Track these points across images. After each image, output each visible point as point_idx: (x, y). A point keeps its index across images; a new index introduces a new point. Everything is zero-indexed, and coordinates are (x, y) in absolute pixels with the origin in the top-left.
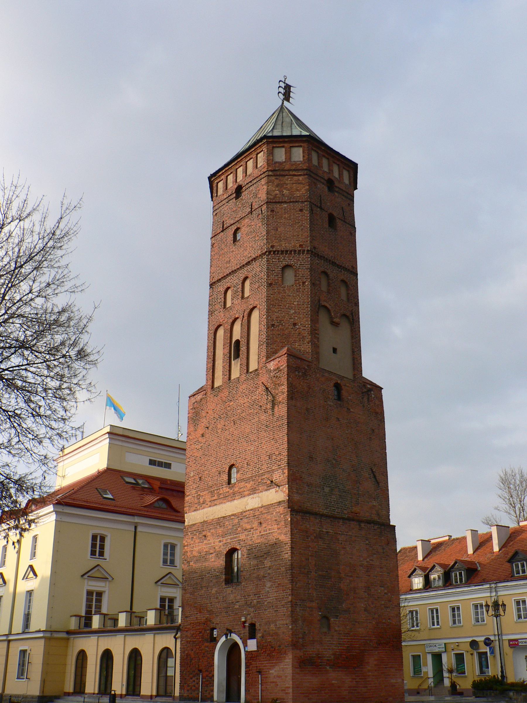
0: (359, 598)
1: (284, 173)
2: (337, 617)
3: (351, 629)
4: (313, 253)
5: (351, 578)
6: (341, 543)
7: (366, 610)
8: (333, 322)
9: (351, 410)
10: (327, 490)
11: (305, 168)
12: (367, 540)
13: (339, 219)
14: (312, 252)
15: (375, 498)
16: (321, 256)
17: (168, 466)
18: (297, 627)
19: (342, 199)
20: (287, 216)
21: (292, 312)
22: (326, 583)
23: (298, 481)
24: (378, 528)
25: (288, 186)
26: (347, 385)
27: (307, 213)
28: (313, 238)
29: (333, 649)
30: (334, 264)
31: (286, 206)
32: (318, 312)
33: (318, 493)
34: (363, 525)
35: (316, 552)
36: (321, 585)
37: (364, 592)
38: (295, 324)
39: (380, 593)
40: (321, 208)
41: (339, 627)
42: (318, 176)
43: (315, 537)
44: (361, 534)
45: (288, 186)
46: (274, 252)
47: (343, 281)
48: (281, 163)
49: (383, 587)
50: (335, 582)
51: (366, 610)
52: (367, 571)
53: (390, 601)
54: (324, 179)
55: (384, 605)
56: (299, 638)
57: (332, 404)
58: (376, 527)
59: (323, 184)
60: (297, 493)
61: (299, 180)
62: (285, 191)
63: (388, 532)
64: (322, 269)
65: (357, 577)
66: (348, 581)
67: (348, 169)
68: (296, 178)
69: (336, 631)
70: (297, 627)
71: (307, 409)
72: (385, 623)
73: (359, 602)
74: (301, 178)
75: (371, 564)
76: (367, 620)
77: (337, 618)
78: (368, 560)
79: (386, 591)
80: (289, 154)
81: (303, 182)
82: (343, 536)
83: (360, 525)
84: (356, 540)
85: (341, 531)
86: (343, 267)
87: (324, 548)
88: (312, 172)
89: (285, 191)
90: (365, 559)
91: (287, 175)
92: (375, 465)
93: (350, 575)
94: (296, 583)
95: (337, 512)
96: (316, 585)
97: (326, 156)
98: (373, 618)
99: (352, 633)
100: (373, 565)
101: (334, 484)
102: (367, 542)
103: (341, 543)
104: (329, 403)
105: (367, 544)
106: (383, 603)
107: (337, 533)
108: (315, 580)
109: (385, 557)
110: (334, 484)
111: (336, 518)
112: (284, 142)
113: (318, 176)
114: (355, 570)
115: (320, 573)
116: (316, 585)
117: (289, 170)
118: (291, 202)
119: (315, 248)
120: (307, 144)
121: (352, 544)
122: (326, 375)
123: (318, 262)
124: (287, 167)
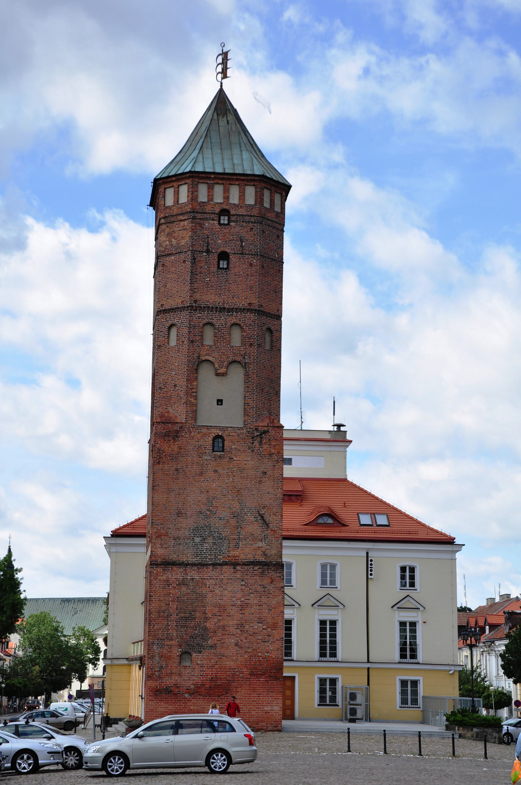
0: (229, 635)
1: (172, 219)
2: (200, 652)
3: (217, 662)
4: (194, 308)
5: (220, 618)
6: (209, 587)
7: (236, 645)
10: (197, 540)
11: (189, 210)
13: (235, 253)
14: (193, 306)
15: (262, 540)
16: (204, 307)
18: (153, 662)
19: (242, 226)
20: (173, 269)
21: (174, 373)
22: (189, 624)
23: (162, 537)
24: (259, 568)
25: (176, 235)
26: (233, 434)
27: (188, 263)
28: (193, 291)
29: (193, 680)
30: (222, 310)
31: (173, 258)
32: (197, 370)
34: (238, 568)
35: (177, 597)
38: (175, 386)
39: (257, 629)
40: (208, 251)
41: (201, 660)
42: (206, 213)
43: (177, 585)
44: (236, 577)
45: (176, 235)
46: (164, 310)
47: (235, 324)
48: (169, 208)
49: (261, 623)
51: (236, 645)
52: (241, 610)
53: (270, 636)
54: (215, 213)
55: (260, 639)
56: (155, 671)
57: (209, 458)
58: (256, 568)
59: (213, 220)
60: (162, 547)
61: (184, 226)
62: (173, 240)
63: (273, 571)
64: (206, 321)
66: (216, 620)
67: (252, 183)
68: (182, 223)
69: (198, 664)
70: (153, 662)
71: (177, 470)
72: (261, 656)
73: (228, 639)
74: (186, 223)
76: (237, 654)
77: (200, 653)
78: (243, 599)
79: (265, 627)
80: (177, 194)
81: (188, 227)
82: (211, 581)
83: (235, 568)
84: (228, 583)
86: (236, 309)
87: (188, 593)
88: (197, 212)
89: (173, 240)
91: (175, 221)
92: (264, 507)
94: (154, 626)
95: (209, 559)
96: (176, 626)
97: (220, 182)
98: (246, 652)
99: (217, 666)
100: (249, 604)
101: (207, 533)
102: (243, 583)
103: (209, 587)
104: (205, 458)
105: (242, 585)
106: (260, 637)
107: (204, 579)
109: (266, 595)
110: (207, 533)
111: (204, 565)
112: (172, 181)
113: (206, 213)
115: (183, 615)
116: (176, 626)
117: (177, 215)
118: (176, 253)
119: (196, 301)
120: (191, 179)
121: (222, 587)
122: (204, 431)
123: (200, 315)
124: (175, 211)
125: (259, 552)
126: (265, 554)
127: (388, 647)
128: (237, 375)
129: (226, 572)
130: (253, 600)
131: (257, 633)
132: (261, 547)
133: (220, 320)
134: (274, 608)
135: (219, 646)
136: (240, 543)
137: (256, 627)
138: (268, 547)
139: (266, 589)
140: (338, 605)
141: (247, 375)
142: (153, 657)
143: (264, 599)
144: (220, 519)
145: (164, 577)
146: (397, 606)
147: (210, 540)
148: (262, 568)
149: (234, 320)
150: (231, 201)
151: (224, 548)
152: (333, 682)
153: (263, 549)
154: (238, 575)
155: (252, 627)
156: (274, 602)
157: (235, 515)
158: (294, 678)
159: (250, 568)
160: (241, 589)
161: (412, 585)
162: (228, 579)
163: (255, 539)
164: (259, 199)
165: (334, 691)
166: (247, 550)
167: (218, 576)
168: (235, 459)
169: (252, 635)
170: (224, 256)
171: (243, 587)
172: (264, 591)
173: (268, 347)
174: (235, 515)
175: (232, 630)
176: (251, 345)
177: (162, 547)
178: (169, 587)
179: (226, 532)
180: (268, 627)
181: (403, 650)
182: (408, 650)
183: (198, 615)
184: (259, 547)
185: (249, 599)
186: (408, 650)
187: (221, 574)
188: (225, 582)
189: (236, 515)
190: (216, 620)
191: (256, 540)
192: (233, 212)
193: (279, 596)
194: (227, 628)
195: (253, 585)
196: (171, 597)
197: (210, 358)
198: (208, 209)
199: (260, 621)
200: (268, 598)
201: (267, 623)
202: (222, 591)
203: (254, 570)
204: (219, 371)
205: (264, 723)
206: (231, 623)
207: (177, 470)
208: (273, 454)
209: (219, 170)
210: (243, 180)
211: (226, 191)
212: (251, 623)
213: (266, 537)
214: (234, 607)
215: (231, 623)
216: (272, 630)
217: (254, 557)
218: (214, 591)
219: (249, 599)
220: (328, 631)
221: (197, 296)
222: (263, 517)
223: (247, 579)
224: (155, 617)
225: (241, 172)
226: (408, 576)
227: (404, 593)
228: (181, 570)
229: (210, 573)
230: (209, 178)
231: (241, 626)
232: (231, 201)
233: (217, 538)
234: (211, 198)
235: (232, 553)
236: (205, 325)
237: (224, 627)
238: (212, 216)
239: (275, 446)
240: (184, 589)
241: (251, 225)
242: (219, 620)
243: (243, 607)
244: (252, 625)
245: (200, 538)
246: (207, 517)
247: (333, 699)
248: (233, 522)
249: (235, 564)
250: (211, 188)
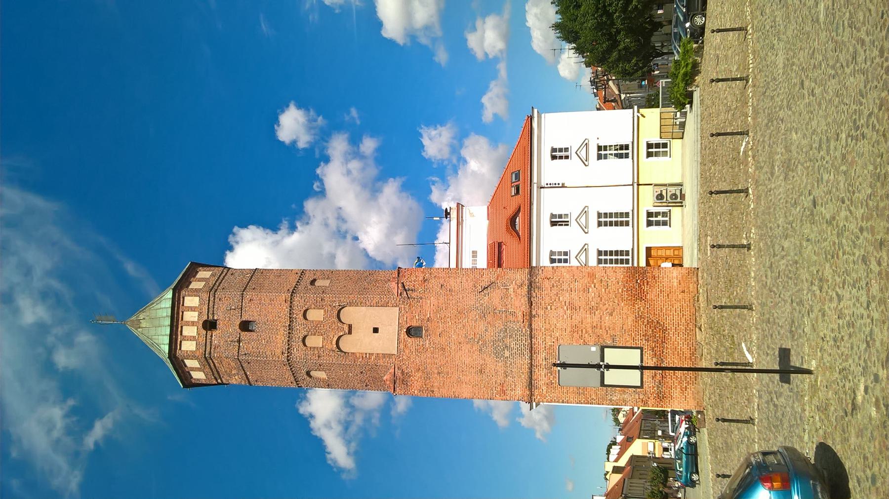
10: (507, 354)
17: (474, 254)
34: (534, 313)
40: (239, 341)
58: (534, 295)
64: (301, 344)
71: (439, 373)
80: (194, 369)
122: (402, 346)
124: (208, 370)
127: (619, 170)
128: (350, 314)
130: (566, 297)
133: (300, 330)
135: (612, 332)
140: (585, 212)
141: (350, 304)
142: (624, 401)
143: (565, 287)
145: (544, 388)
146: (585, 162)
147: (508, 340)
149: (301, 316)
150: (196, 319)
152: (649, 214)
154: (541, 312)
156: (568, 276)
157: (483, 316)
158: (649, 249)
161: (566, 149)
163: (506, 296)
164: (196, 292)
165: (657, 214)
166: (517, 304)
170: (245, 326)
173: (326, 283)
174: (483, 316)
175: (596, 319)
179: (499, 325)
181: (620, 156)
182: (622, 152)
186: (622, 152)
188: (548, 326)
192: (205, 318)
197: (335, 339)
198: (202, 340)
199: (586, 290)
204: (347, 331)
205: (691, 286)
206: (589, 320)
207: (439, 373)
209: (168, 332)
210: (178, 308)
211: (188, 324)
213: (505, 285)
215: (589, 320)
220: (608, 220)
225: (170, 310)
226: (558, 154)
227: (574, 156)
229: (539, 341)
231: (592, 310)
232: (196, 319)
234: (192, 338)
235: (520, 318)
236: (305, 345)
237: (593, 327)
238: (209, 337)
242: (586, 332)
243: (572, 307)
246: (484, 344)
247: (664, 214)
248: (489, 318)
249: (531, 316)
250: (186, 338)
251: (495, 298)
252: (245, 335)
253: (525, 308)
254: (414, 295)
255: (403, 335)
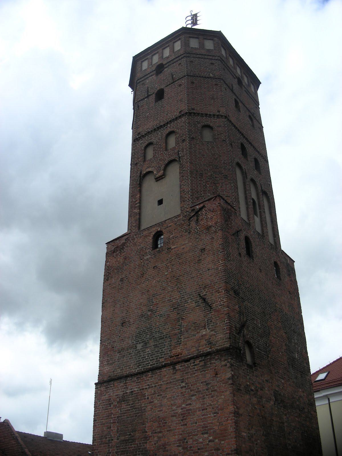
4: (139, 139)
5: (160, 435)
6: (148, 398)
8: (158, 178)
9: (173, 247)
10: (139, 346)
12: (182, 382)
15: (205, 326)
22: (129, 448)
24: (200, 361)
33: (130, 354)
34: (178, 367)
36: (122, 451)
37: (178, 446)
39: (202, 443)
43: (118, 402)
44: (175, 378)
49: (207, 433)
50: (140, 444)
52: (182, 420)
58: (197, 362)
63: (216, 360)
65: (168, 431)
66: (156, 439)
75: (187, 410)
78: (184, 406)
79: (211, 438)
82: (150, 390)
83: (174, 368)
85: (148, 385)
87: (127, 410)
90: (179, 406)
93: (159, 430)
100: (190, 410)
101: (148, 336)
102: (184, 384)
103: (148, 398)
105: (182, 388)
107: (143, 389)
108: (117, 447)
109: (210, 394)
114: (166, 423)
125: (204, 342)
126: (210, 343)
129: (165, 376)
131: (202, 449)
132: (205, 335)
134: (222, 409)
136: (182, 337)
137: (201, 440)
138: (213, 333)
139: (209, 386)
144: (161, 316)
147: (152, 343)
148: (203, 360)
151: (166, 348)
153: (207, 337)
154: (178, 376)
155: (197, 440)
157: (176, 307)
159: (190, 364)
160: (182, 393)
162: (167, 383)
167: (157, 383)
168: (173, 247)
169: (197, 452)
171: (184, 390)
172: (207, 389)
174: (176, 307)
176: (184, 140)
177: (108, 364)
178: (110, 406)
180: (215, 438)
183: (137, 435)
184: (202, 336)
185: (190, 404)
187: (160, 380)
189: (176, 306)
190: (156, 439)
191: (198, 329)
193: (226, 391)
194: (168, 448)
195: (195, 384)
196: (112, 418)
199: (205, 430)
200: (212, 397)
201: (214, 432)
202: (161, 400)
203: (195, 365)
207: (122, 280)
208: (210, 227)
212: (194, 435)
214: (174, 418)
216: (221, 440)
217: (198, 350)
218: (152, 402)
219: (190, 404)
221: (140, 130)
222: (204, 299)
223: (188, 378)
224: (98, 445)
228: (122, 384)
230: (148, 54)
233: (158, 339)
239: (212, 218)
240: (124, 406)
241: (179, 62)
242: (159, 438)
243: (185, 416)
244: (196, 437)
245: (142, 344)
251: (196, 315)
252: (153, 98)
253: (186, 354)
254: (193, 224)
255: (154, 231)
